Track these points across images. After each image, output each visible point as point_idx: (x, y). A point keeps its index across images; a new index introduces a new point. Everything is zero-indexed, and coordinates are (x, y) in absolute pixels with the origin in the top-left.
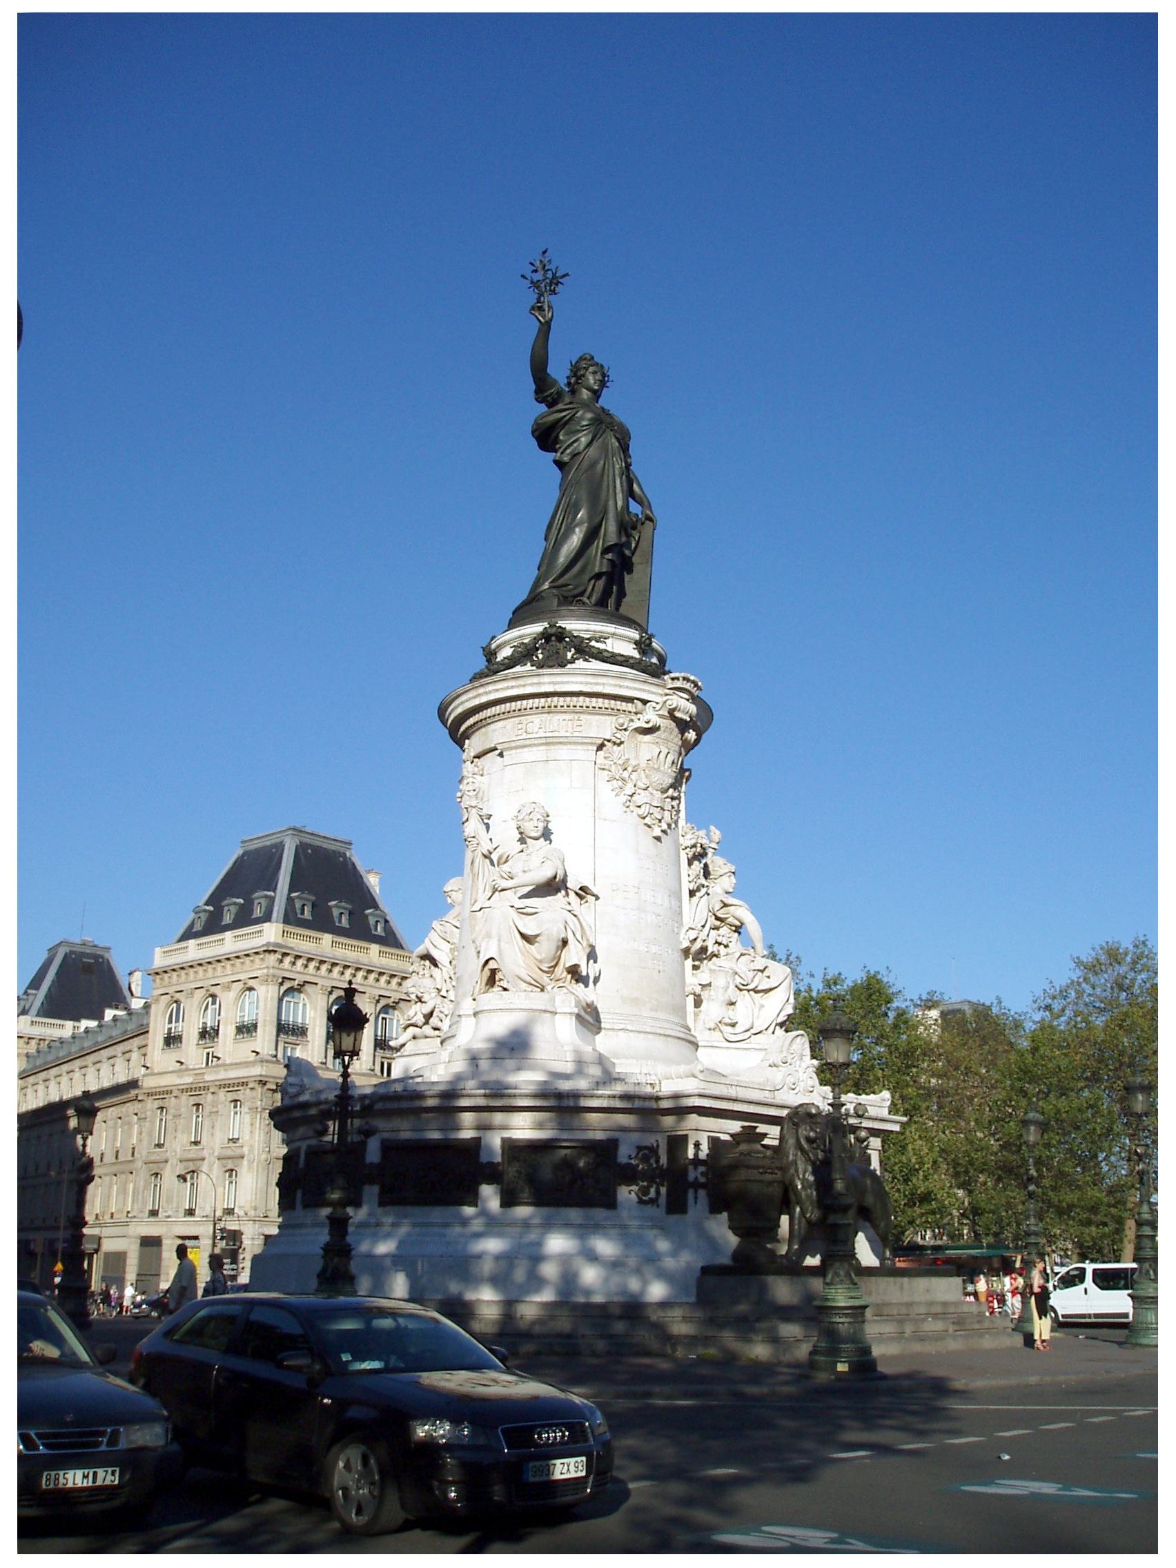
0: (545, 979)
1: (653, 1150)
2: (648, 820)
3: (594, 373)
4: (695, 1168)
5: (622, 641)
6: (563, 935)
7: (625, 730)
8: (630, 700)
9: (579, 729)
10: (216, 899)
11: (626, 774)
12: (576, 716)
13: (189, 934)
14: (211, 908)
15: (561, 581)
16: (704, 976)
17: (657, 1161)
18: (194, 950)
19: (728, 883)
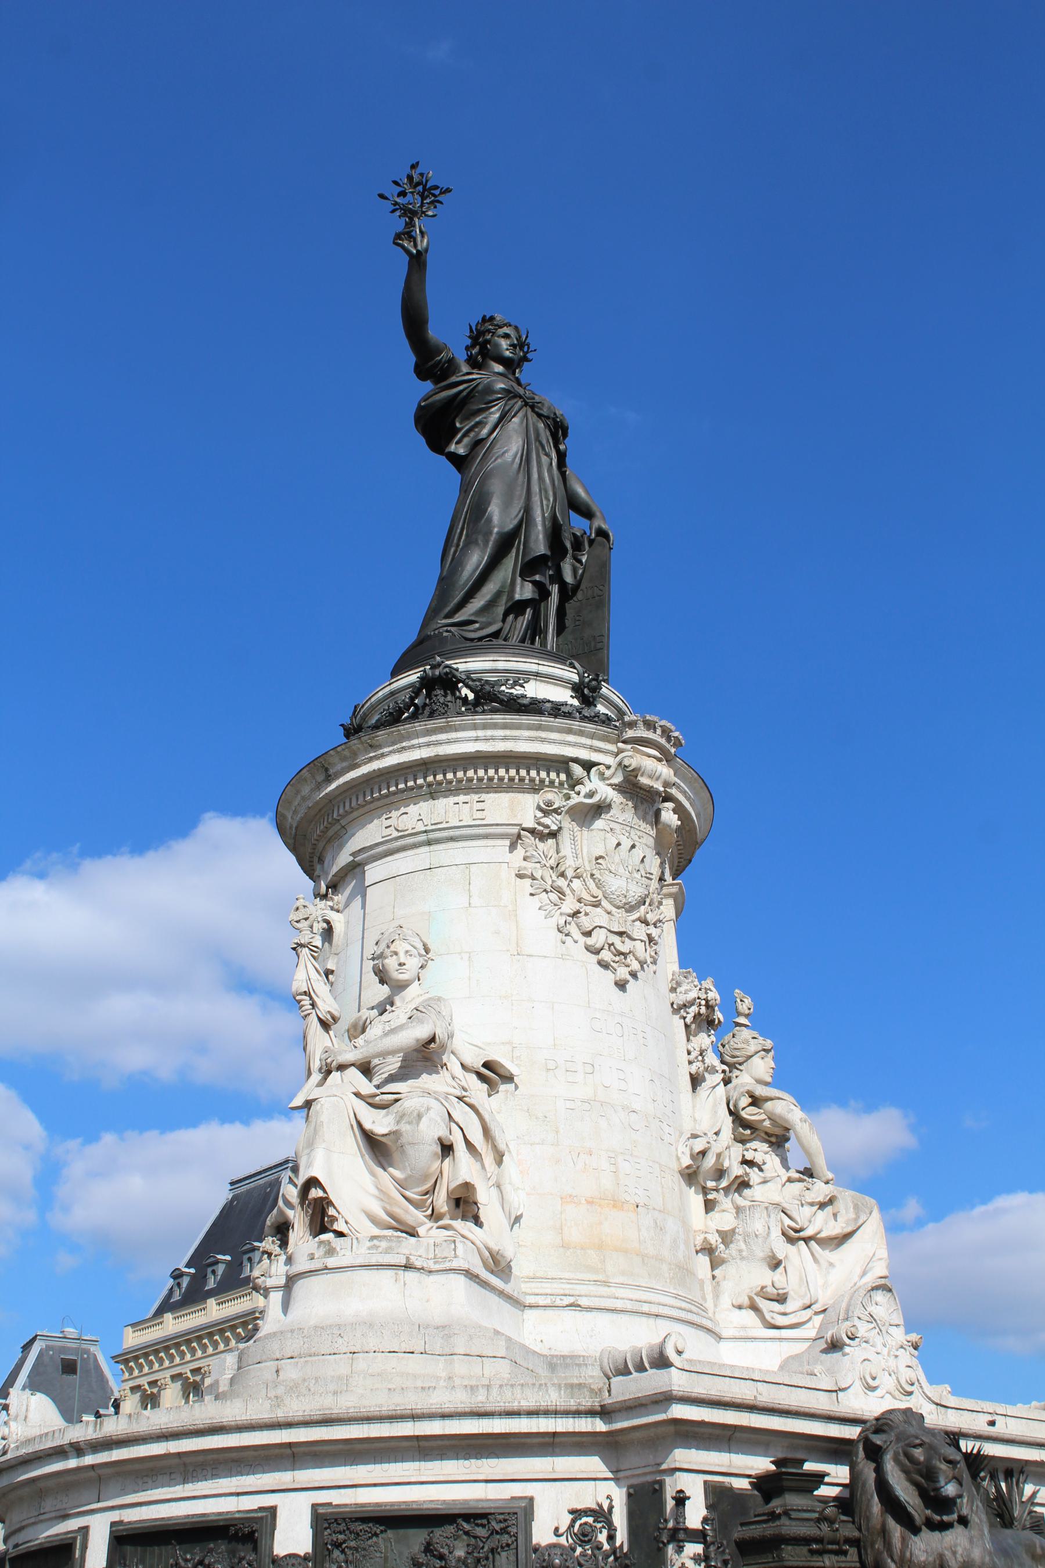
0: (415, 1216)
1: (603, 1515)
2: (606, 955)
3: (506, 336)
4: (680, 1550)
5: (550, 683)
6: (442, 1132)
7: (556, 811)
8: (562, 764)
9: (479, 815)
10: (201, 1259)
11: (562, 883)
12: (475, 797)
13: (167, 1306)
14: (192, 1271)
15: (458, 618)
16: (724, 1219)
17: (611, 1538)
18: (172, 1325)
19: (762, 1067)
